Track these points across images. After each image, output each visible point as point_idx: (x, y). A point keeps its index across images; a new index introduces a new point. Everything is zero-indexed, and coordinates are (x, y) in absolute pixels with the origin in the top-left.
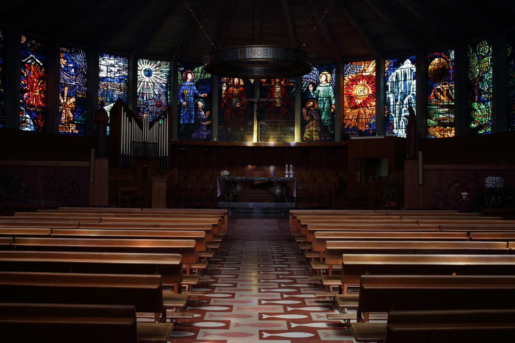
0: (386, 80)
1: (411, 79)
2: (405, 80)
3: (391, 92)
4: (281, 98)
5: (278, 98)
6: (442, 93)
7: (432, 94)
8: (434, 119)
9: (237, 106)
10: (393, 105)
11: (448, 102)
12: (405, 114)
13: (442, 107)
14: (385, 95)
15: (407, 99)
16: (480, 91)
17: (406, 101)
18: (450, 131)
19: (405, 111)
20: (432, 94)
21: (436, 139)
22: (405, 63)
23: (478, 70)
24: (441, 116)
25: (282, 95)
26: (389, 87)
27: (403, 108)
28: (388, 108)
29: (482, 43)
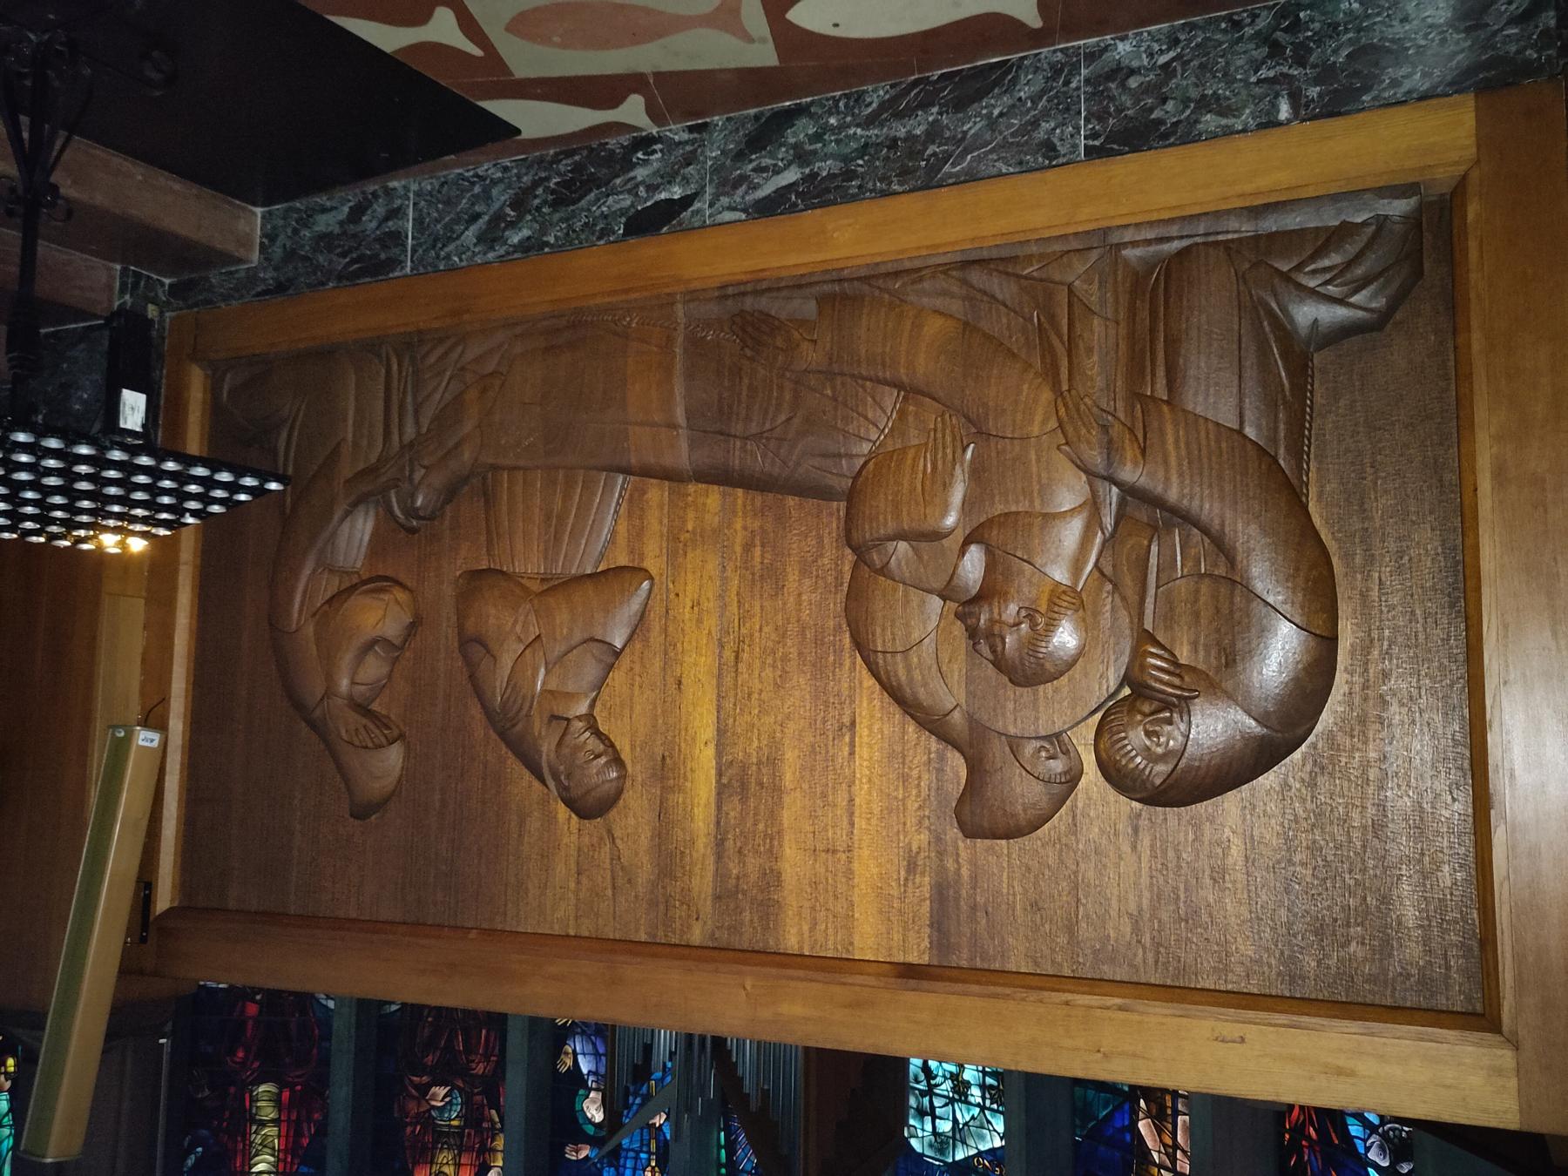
4: (253, 1120)
5: (263, 1124)
9: (441, 1091)
25: (245, 1135)
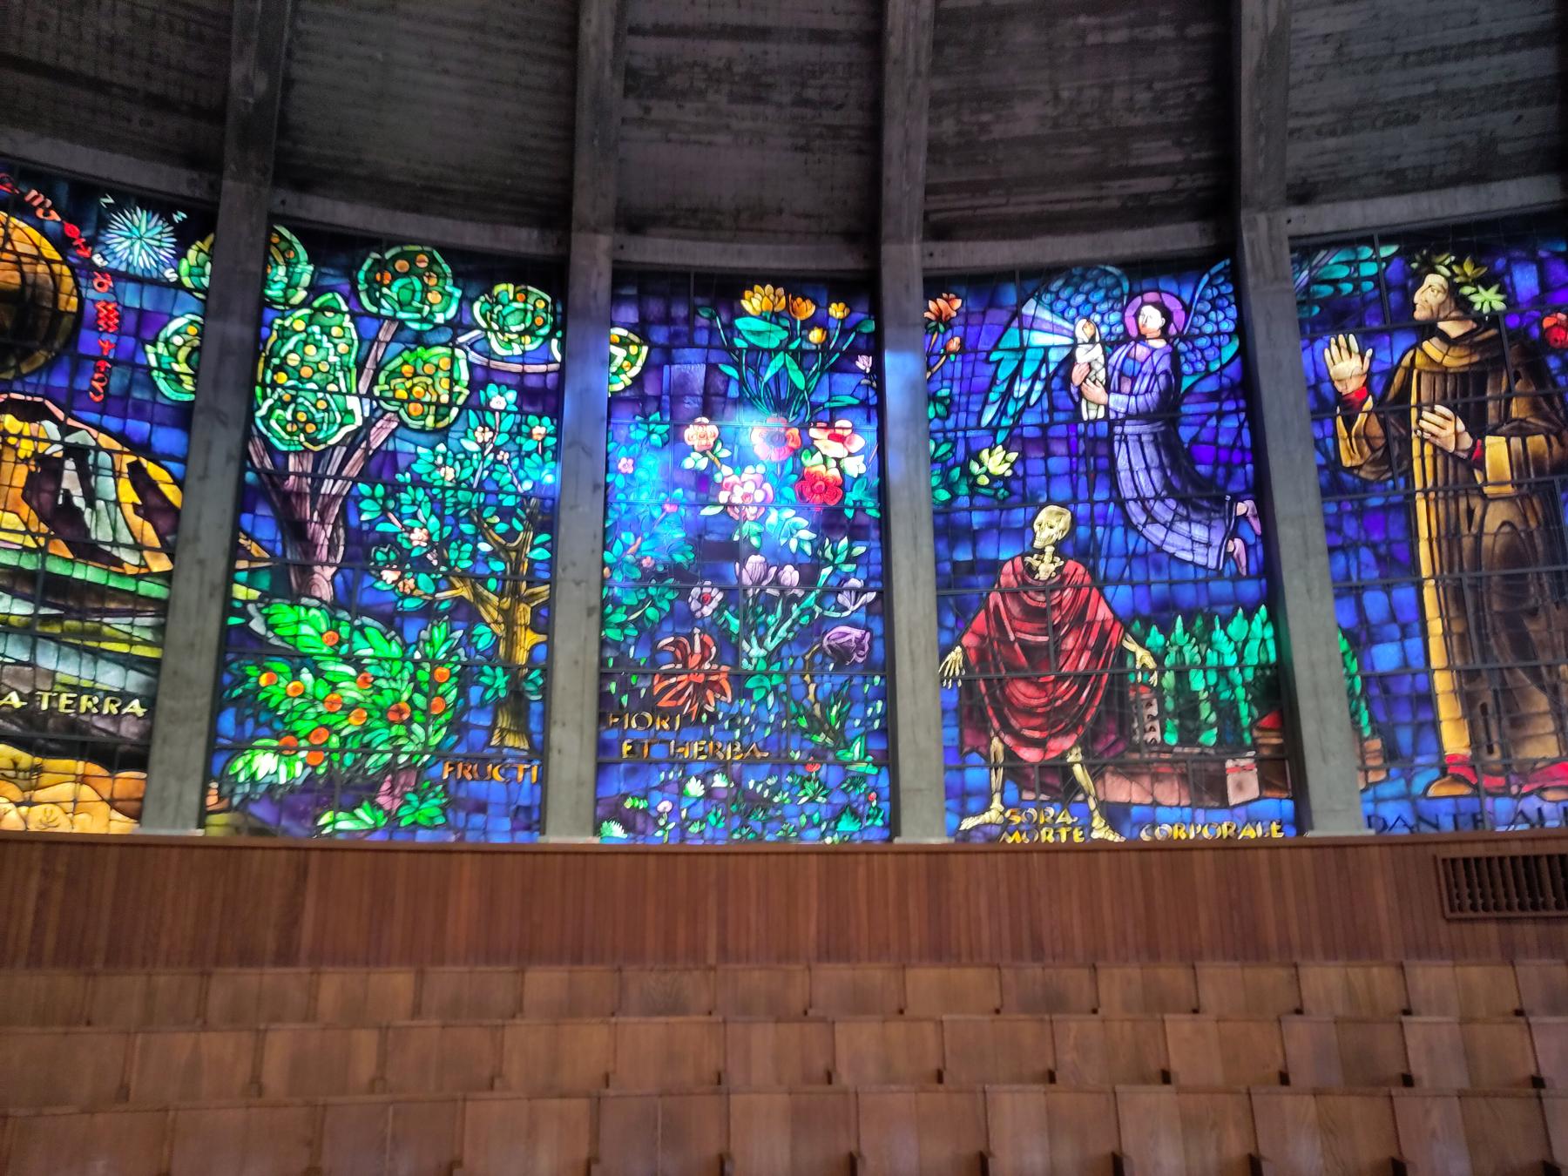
11: (42, 551)
16: (361, 547)
23: (353, 403)
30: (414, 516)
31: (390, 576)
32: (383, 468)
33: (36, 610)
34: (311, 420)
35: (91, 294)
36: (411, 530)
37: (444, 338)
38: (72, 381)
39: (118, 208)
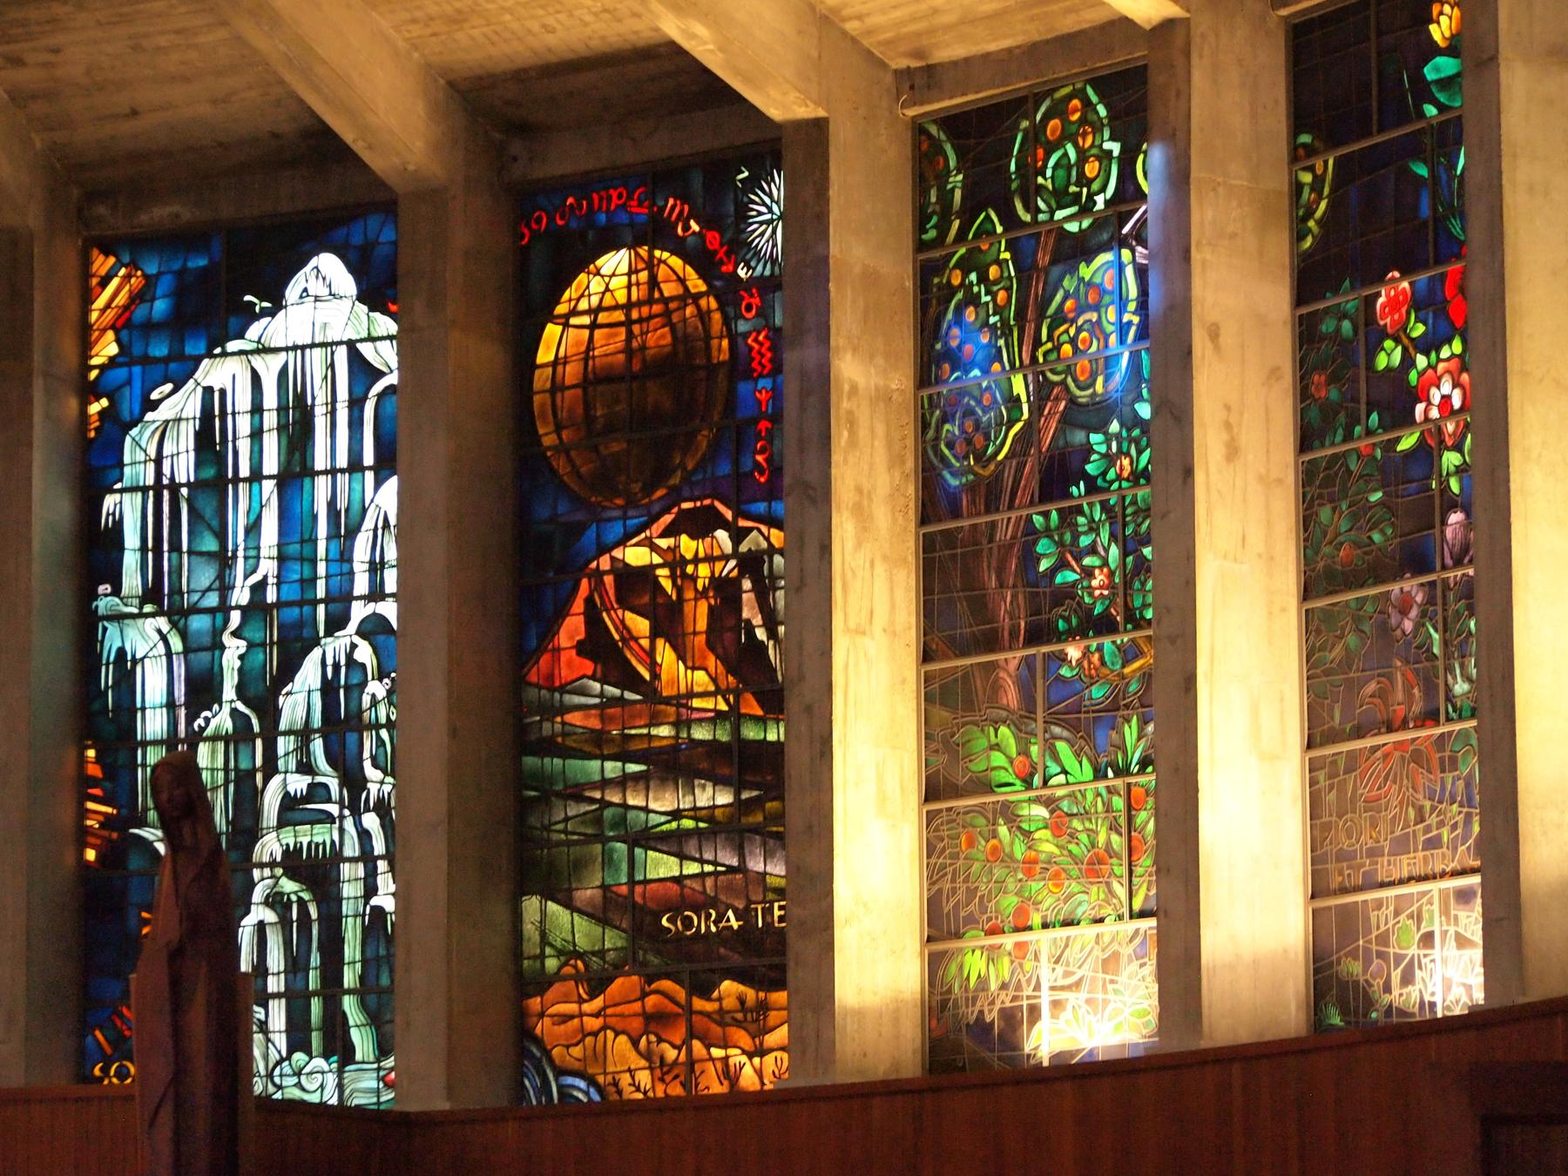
0: (96, 465)
1: (355, 466)
2: (296, 472)
3: (152, 594)
6: (668, 622)
7: (572, 628)
8: (587, 893)
10: (171, 741)
11: (734, 716)
12: (288, 837)
13: (674, 765)
14: (88, 627)
15: (309, 675)
17: (300, 700)
18: (755, 1019)
19: (290, 803)
20: (572, 628)
21: (613, 1108)
22: (292, 293)
24: (661, 866)
26: (131, 539)
27: (270, 769)
28: (110, 771)
29: (1059, 110)
30: (1092, 550)
31: (1073, 652)
32: (1060, 474)
33: (737, 794)
34: (977, 425)
35: (742, 327)
36: (1088, 573)
37: (1105, 236)
38: (737, 463)
39: (753, 184)
